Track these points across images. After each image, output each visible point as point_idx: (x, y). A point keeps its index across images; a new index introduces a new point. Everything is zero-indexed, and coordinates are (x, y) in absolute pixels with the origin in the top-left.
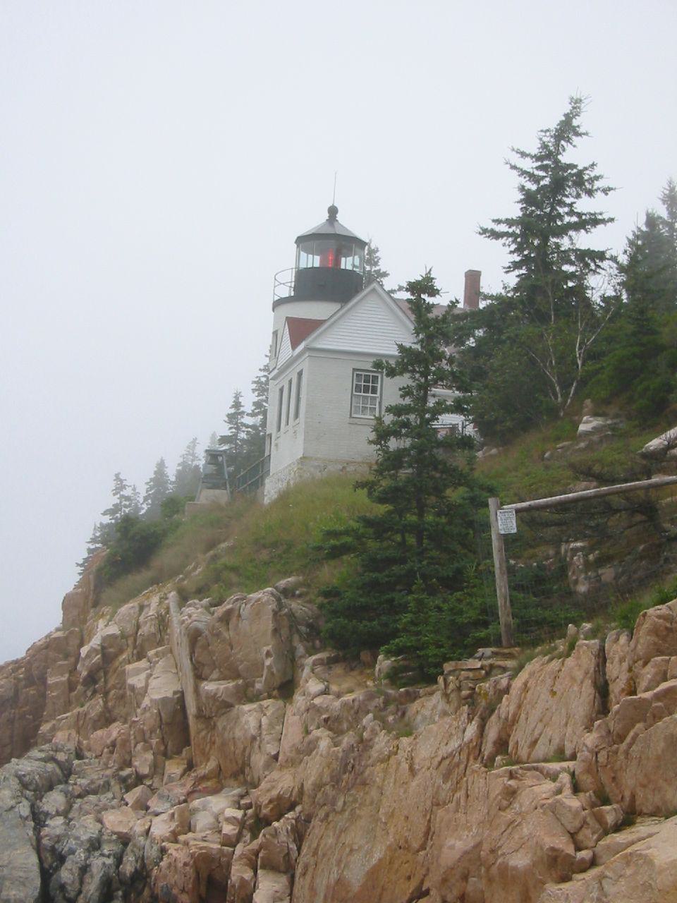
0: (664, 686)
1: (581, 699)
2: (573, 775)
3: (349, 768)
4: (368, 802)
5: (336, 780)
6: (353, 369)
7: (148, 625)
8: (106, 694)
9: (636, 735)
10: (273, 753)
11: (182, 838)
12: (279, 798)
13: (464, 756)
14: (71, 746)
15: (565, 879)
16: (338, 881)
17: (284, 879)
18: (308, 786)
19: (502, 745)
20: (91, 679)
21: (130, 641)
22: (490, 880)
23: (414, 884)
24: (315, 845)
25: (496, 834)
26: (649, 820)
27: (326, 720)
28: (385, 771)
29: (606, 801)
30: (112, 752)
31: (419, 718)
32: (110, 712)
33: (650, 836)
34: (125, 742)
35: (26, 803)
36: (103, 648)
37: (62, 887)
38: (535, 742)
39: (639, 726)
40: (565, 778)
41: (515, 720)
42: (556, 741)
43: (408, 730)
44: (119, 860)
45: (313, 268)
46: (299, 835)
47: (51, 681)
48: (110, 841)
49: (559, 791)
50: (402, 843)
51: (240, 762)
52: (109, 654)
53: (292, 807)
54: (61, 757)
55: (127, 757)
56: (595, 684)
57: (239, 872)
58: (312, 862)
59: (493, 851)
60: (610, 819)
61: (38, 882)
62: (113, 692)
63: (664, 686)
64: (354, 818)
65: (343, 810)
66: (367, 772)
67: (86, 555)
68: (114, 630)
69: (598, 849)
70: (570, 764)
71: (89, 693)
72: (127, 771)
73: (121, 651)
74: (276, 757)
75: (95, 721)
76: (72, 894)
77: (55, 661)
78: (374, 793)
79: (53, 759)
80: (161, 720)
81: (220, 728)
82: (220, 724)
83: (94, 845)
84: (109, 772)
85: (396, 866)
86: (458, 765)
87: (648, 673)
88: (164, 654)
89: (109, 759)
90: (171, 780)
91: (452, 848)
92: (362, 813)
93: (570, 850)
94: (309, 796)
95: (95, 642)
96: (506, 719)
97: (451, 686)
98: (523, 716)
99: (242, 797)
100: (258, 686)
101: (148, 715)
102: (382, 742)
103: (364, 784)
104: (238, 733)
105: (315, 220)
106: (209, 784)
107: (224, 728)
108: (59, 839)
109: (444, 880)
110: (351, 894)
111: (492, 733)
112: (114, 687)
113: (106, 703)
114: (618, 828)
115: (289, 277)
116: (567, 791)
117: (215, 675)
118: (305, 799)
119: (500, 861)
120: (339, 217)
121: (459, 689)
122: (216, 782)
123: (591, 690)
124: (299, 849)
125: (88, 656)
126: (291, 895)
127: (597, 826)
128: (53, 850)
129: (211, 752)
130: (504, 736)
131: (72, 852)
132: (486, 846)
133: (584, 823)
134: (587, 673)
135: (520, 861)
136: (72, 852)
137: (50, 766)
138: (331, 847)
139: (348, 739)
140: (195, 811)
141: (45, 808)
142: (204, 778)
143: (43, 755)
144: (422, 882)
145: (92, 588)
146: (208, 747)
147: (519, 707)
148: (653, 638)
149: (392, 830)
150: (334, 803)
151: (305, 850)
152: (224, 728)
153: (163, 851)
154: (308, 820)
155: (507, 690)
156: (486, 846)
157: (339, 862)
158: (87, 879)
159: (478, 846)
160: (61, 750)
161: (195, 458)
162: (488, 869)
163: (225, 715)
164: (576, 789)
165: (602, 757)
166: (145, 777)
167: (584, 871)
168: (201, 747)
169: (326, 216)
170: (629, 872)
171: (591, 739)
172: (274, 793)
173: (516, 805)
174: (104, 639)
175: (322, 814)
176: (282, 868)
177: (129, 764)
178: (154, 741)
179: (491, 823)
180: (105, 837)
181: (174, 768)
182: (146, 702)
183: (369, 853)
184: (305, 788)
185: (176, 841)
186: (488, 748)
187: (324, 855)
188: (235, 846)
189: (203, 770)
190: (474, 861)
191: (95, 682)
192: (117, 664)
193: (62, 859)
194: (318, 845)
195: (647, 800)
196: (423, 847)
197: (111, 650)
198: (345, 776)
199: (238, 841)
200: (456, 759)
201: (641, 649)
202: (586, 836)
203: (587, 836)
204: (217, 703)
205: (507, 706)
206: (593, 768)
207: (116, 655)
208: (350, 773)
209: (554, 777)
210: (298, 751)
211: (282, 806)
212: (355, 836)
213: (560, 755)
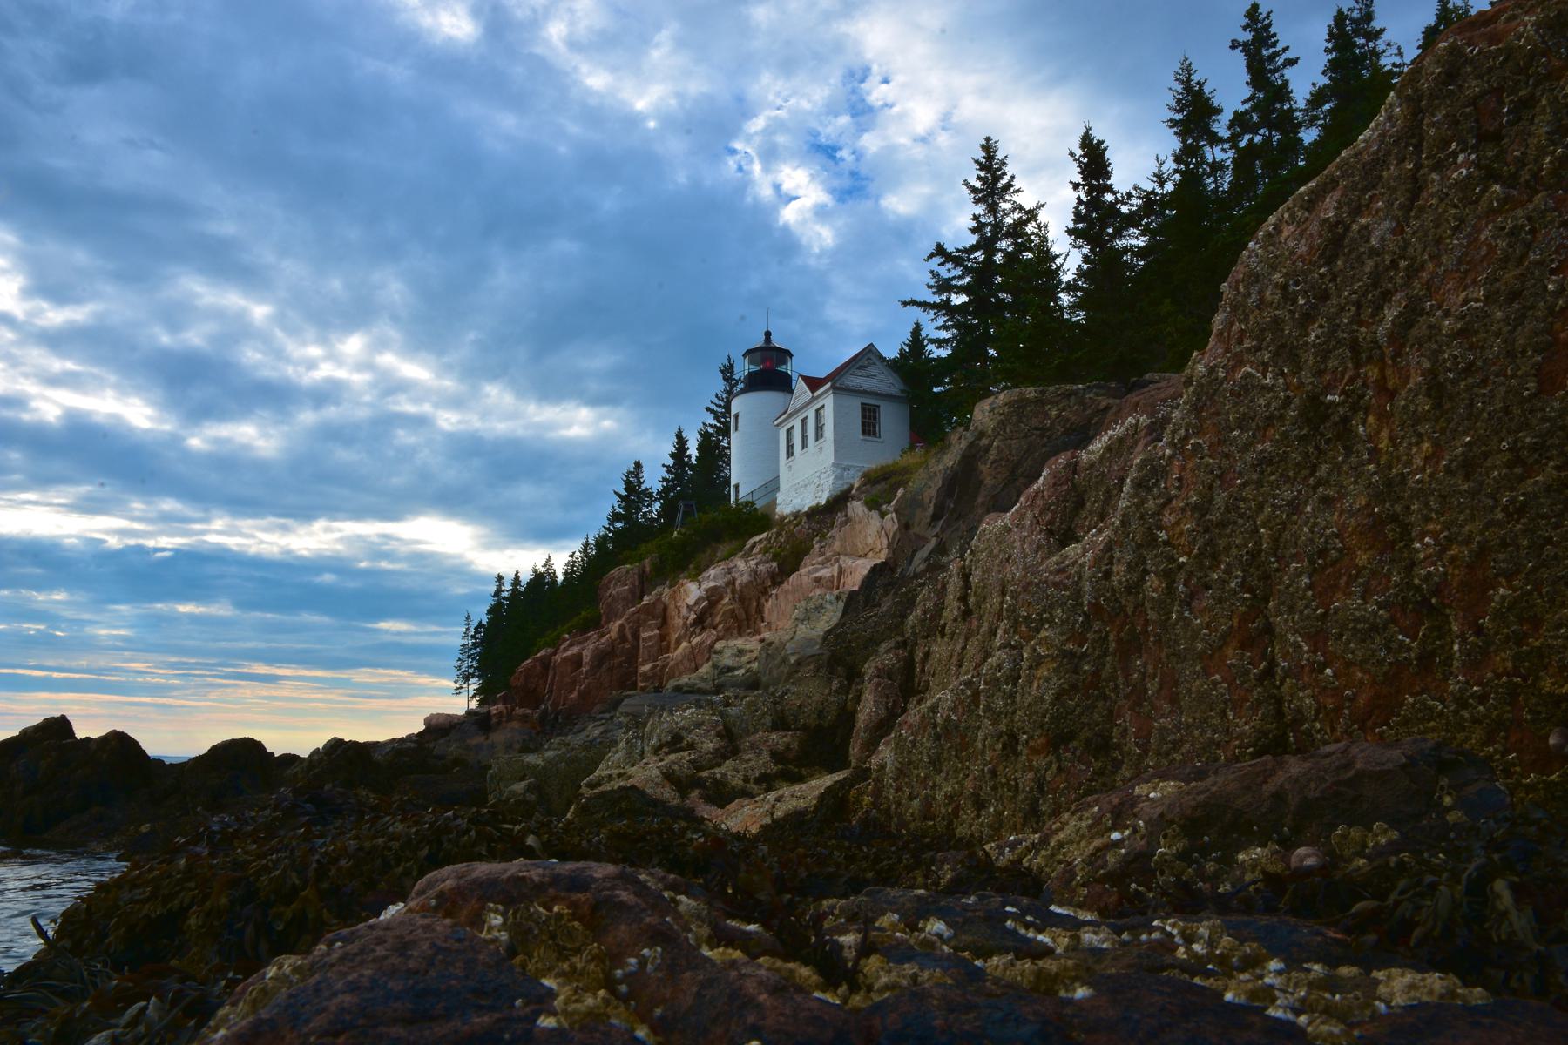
47: (644, 635)
52: (713, 596)
73: (721, 598)
105: (759, 341)
125: (696, 603)
207: (717, 602)
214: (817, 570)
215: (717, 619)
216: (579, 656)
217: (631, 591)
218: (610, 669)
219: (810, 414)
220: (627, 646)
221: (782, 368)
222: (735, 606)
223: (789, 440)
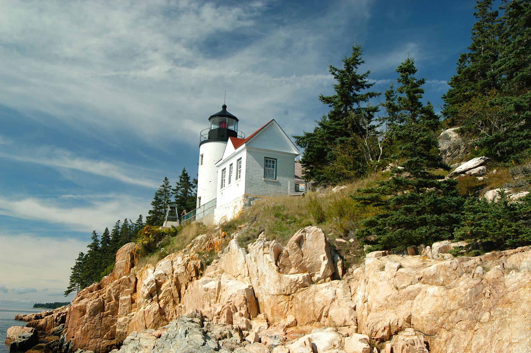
3: (487, 295)
4: (519, 311)
6: (265, 158)
7: (180, 268)
20: (150, 296)
27: (420, 279)
30: (218, 318)
36: (156, 280)
47: (122, 298)
51: (318, 315)
64: (503, 324)
66: (510, 295)
67: (75, 265)
68: (159, 271)
71: (149, 301)
73: (165, 281)
74: (355, 309)
77: (123, 289)
80: (246, 300)
81: (300, 299)
104: (317, 299)
112: (162, 298)
117: (293, 270)
120: (227, 109)
129: (288, 313)
138: (485, 343)
142: (288, 327)
145: (130, 259)
146: (286, 310)
152: (304, 298)
161: (119, 228)
163: (303, 292)
166: (244, 329)
168: (280, 311)
172: (386, 324)
178: (243, 311)
197: (160, 281)
204: (298, 285)
214: (206, 282)
218: (101, 318)
219: (234, 161)
220: (112, 303)
221: (231, 128)
222: (173, 287)
223: (223, 176)
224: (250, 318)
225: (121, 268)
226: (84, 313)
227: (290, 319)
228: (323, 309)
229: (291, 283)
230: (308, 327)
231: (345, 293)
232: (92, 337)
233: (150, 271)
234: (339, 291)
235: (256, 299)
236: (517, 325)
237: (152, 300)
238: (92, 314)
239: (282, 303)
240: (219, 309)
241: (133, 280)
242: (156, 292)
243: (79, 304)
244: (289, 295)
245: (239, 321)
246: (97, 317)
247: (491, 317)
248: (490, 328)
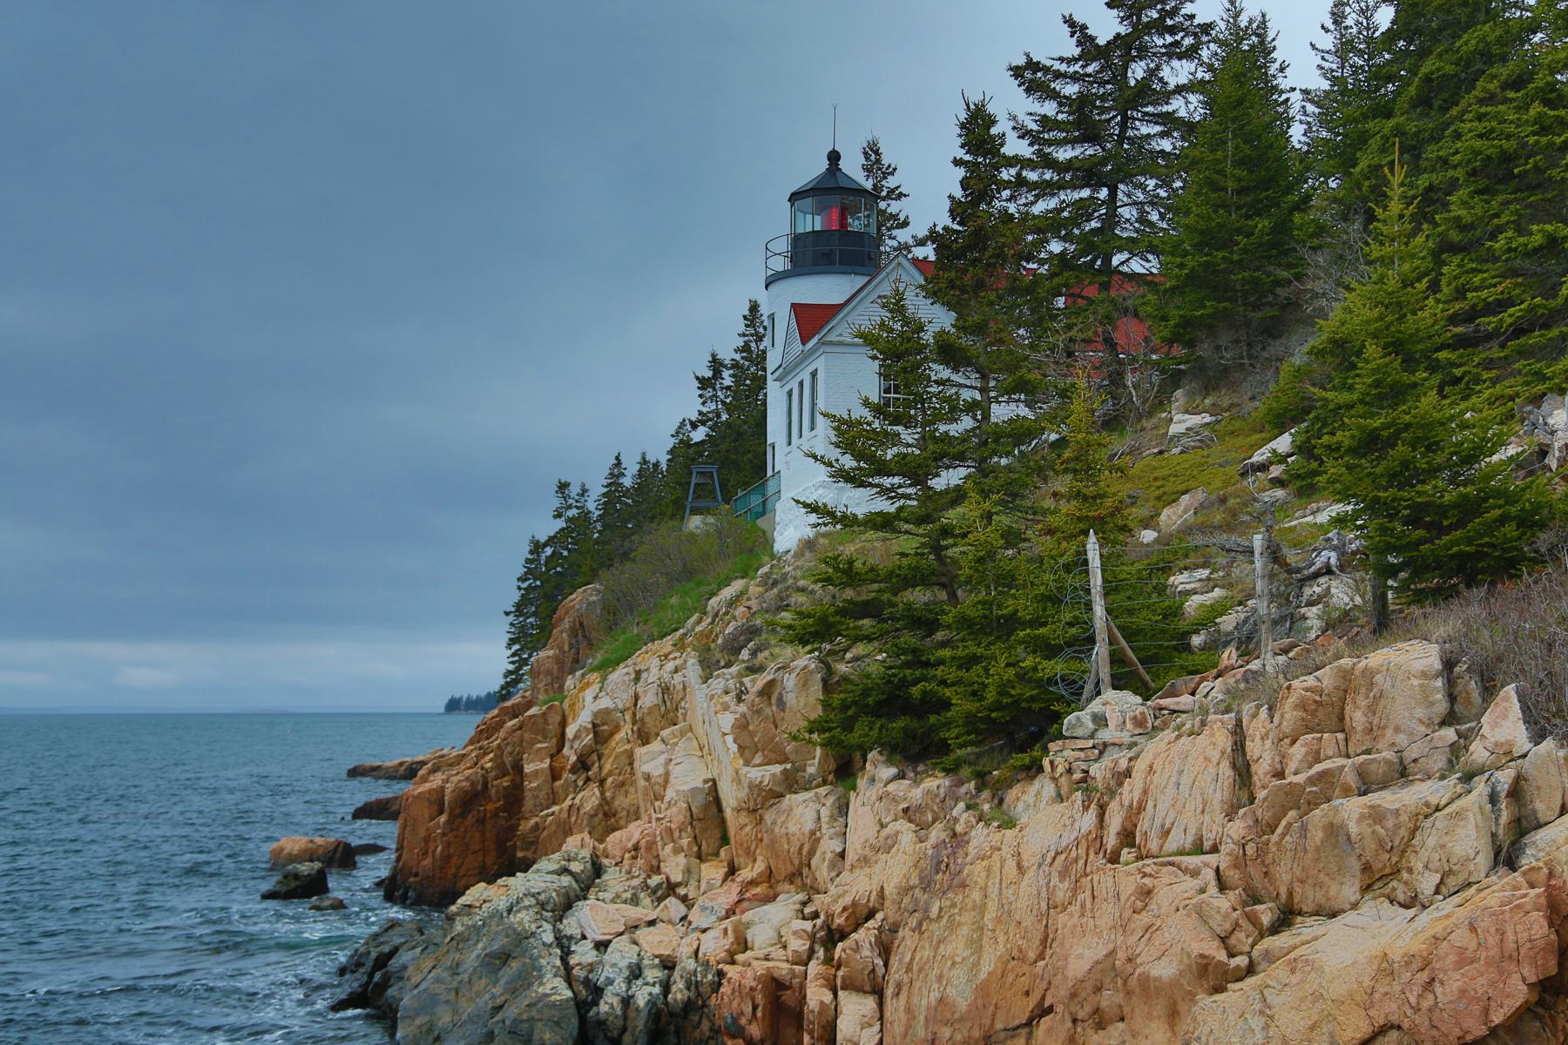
0: (1318, 768)
1: (1217, 781)
2: (1217, 870)
5: (926, 884)
8: (602, 782)
9: (1289, 825)
10: (839, 850)
11: (740, 957)
12: (854, 904)
13: (1082, 851)
14: (586, 853)
15: (1218, 989)
16: (941, 1000)
17: (870, 1003)
18: (889, 890)
19: (1127, 837)
20: (583, 765)
21: (628, 717)
22: (1128, 993)
23: (1032, 1001)
24: (907, 959)
25: (1132, 940)
26: (1310, 920)
27: (906, 810)
28: (989, 870)
29: (1257, 900)
30: (635, 858)
31: (1020, 806)
32: (608, 803)
33: (1316, 939)
34: (651, 845)
35: (547, 927)
36: (595, 725)
37: (601, 1023)
38: (1168, 832)
39: (1292, 814)
40: (1209, 875)
41: (1141, 808)
42: (1192, 831)
43: (1009, 823)
44: (666, 987)
45: (814, 232)
46: (885, 950)
47: (528, 768)
48: (654, 966)
49: (1203, 891)
50: (1015, 953)
51: (796, 862)
52: (601, 731)
53: (871, 915)
54: (576, 867)
55: (655, 863)
56: (1234, 766)
57: (817, 996)
58: (906, 980)
59: (1130, 960)
60: (1266, 919)
61: (575, 1021)
62: (610, 780)
63: (1318, 768)
64: (953, 926)
65: (939, 917)
68: (605, 703)
69: (1255, 954)
70: (1212, 859)
71: (580, 783)
72: (655, 880)
73: (617, 729)
74: (842, 855)
75: (592, 816)
76: (615, 1034)
78: (976, 895)
79: (565, 871)
82: (769, 817)
83: (636, 972)
84: (635, 882)
85: (1010, 980)
86: (1076, 860)
87: (1298, 752)
88: (682, 734)
89: (631, 866)
90: (710, 887)
91: (1080, 956)
92: (963, 920)
93: (1222, 956)
94: (893, 902)
95: (584, 719)
96: (1131, 806)
97: (1060, 769)
98: (1150, 805)
99: (804, 904)
100: (811, 770)
101: (674, 810)
102: (981, 837)
103: (963, 885)
104: (793, 828)
106: (758, 890)
107: (774, 823)
108: (591, 967)
109: (1073, 995)
110: (957, 1016)
111: (1115, 823)
112: (610, 773)
113: (602, 793)
114: (1275, 930)
115: (783, 245)
116: (1213, 889)
117: (758, 759)
118: (887, 903)
119: (1138, 971)
120: (842, 164)
121: (1069, 771)
122: (768, 887)
123: (1230, 772)
124: (886, 965)
125: (576, 737)
126: (881, 1018)
127: (1251, 928)
128: (586, 981)
130: (1129, 827)
131: (610, 982)
132: (1121, 955)
133: (1236, 926)
134: (1223, 753)
135: (1164, 970)
136: (610, 982)
137: (566, 880)
139: (937, 833)
140: (748, 925)
141: (569, 932)
143: (556, 867)
144: (1043, 998)
147: (1145, 792)
148: (1299, 714)
149: (1001, 939)
150: (926, 910)
151: (894, 962)
152: (774, 823)
153: (721, 974)
154: (894, 929)
155: (1128, 773)
156: (1121, 955)
157: (940, 978)
158: (632, 1014)
159: (1113, 952)
160: (575, 859)
162: (1125, 982)
164: (1222, 886)
165: (1251, 849)
166: (678, 885)
167: (1241, 979)
169: (825, 164)
170: (1295, 979)
171: (1237, 829)
172: (848, 900)
173: (1153, 906)
174: (596, 715)
175: (913, 922)
176: (868, 988)
177: (658, 870)
178: (685, 842)
179: (1124, 927)
180: (646, 962)
181: (712, 872)
182: (670, 794)
183: (976, 965)
184: (887, 892)
185: (733, 962)
186: (1111, 841)
187: (920, 970)
188: (806, 965)
189: (746, 874)
190: (1108, 971)
191: (587, 768)
192: (613, 744)
193: (598, 992)
194: (912, 959)
195: (1307, 897)
196: (1041, 957)
198: (939, 876)
199: (810, 958)
200: (1074, 854)
201: (1287, 726)
202: (1239, 940)
203: (1242, 939)
205: (1130, 791)
206: (1240, 862)
207: (612, 734)
208: (942, 872)
209: (1195, 873)
210: (872, 847)
211: (861, 915)
212: (957, 946)
213: (1198, 848)
215: (607, 767)
216: (442, 789)
217: (559, 661)
218: (481, 822)
224: (699, 857)
225: (549, 672)
226: (441, 813)
227: (760, 866)
228: (801, 848)
229: (750, 787)
230: (787, 886)
231: (833, 818)
232: (462, 873)
233: (588, 695)
234: (825, 813)
235: (720, 809)
236: (965, 930)
237: (588, 779)
238: (457, 811)
239: (748, 829)
240: (636, 837)
241: (555, 719)
242: (594, 757)
243: (427, 786)
244: (755, 811)
245: (674, 867)
246: (470, 819)
247: (941, 909)
248: (936, 929)
